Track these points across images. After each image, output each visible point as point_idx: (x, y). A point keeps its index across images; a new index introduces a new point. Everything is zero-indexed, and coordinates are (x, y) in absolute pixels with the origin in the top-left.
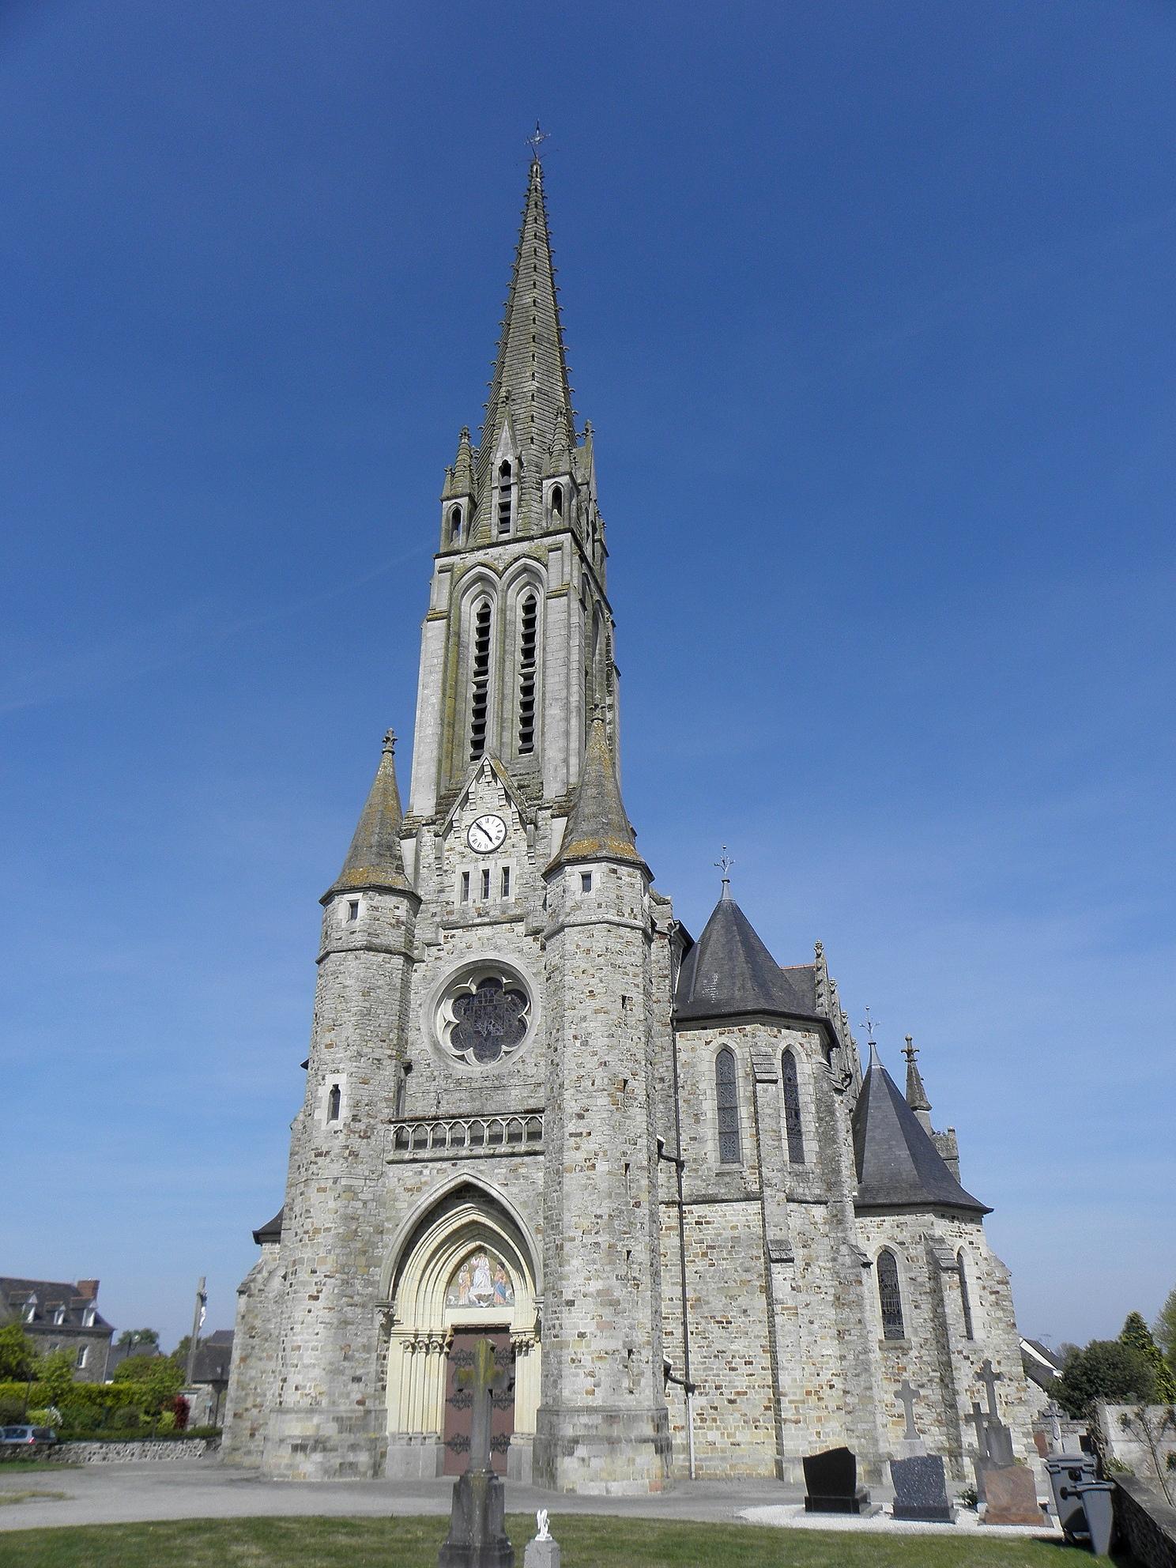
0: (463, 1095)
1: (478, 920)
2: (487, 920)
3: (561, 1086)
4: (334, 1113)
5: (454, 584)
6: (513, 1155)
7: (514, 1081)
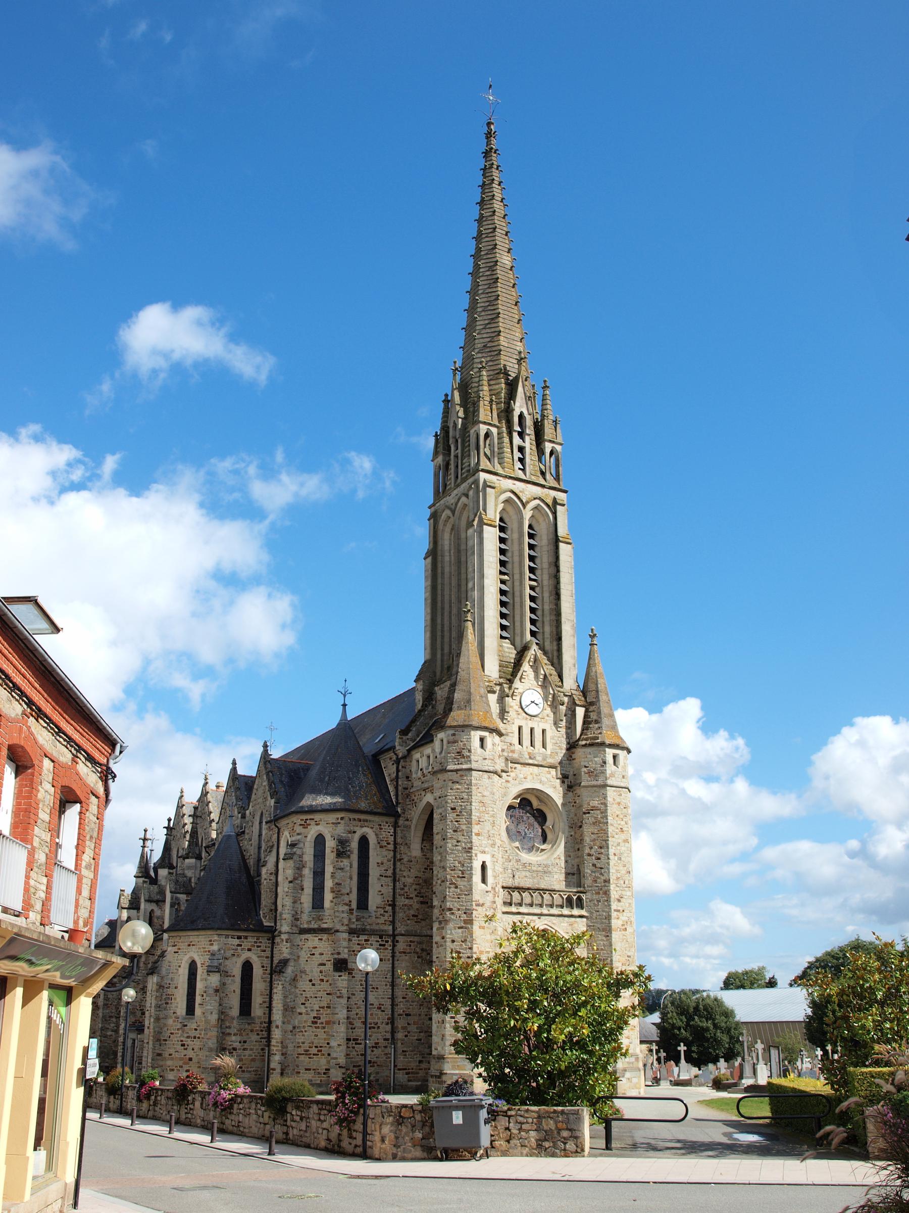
0: (528, 874)
1: (531, 761)
2: (536, 763)
3: (607, 881)
4: (484, 880)
5: (497, 498)
6: (572, 916)
7: (555, 870)
